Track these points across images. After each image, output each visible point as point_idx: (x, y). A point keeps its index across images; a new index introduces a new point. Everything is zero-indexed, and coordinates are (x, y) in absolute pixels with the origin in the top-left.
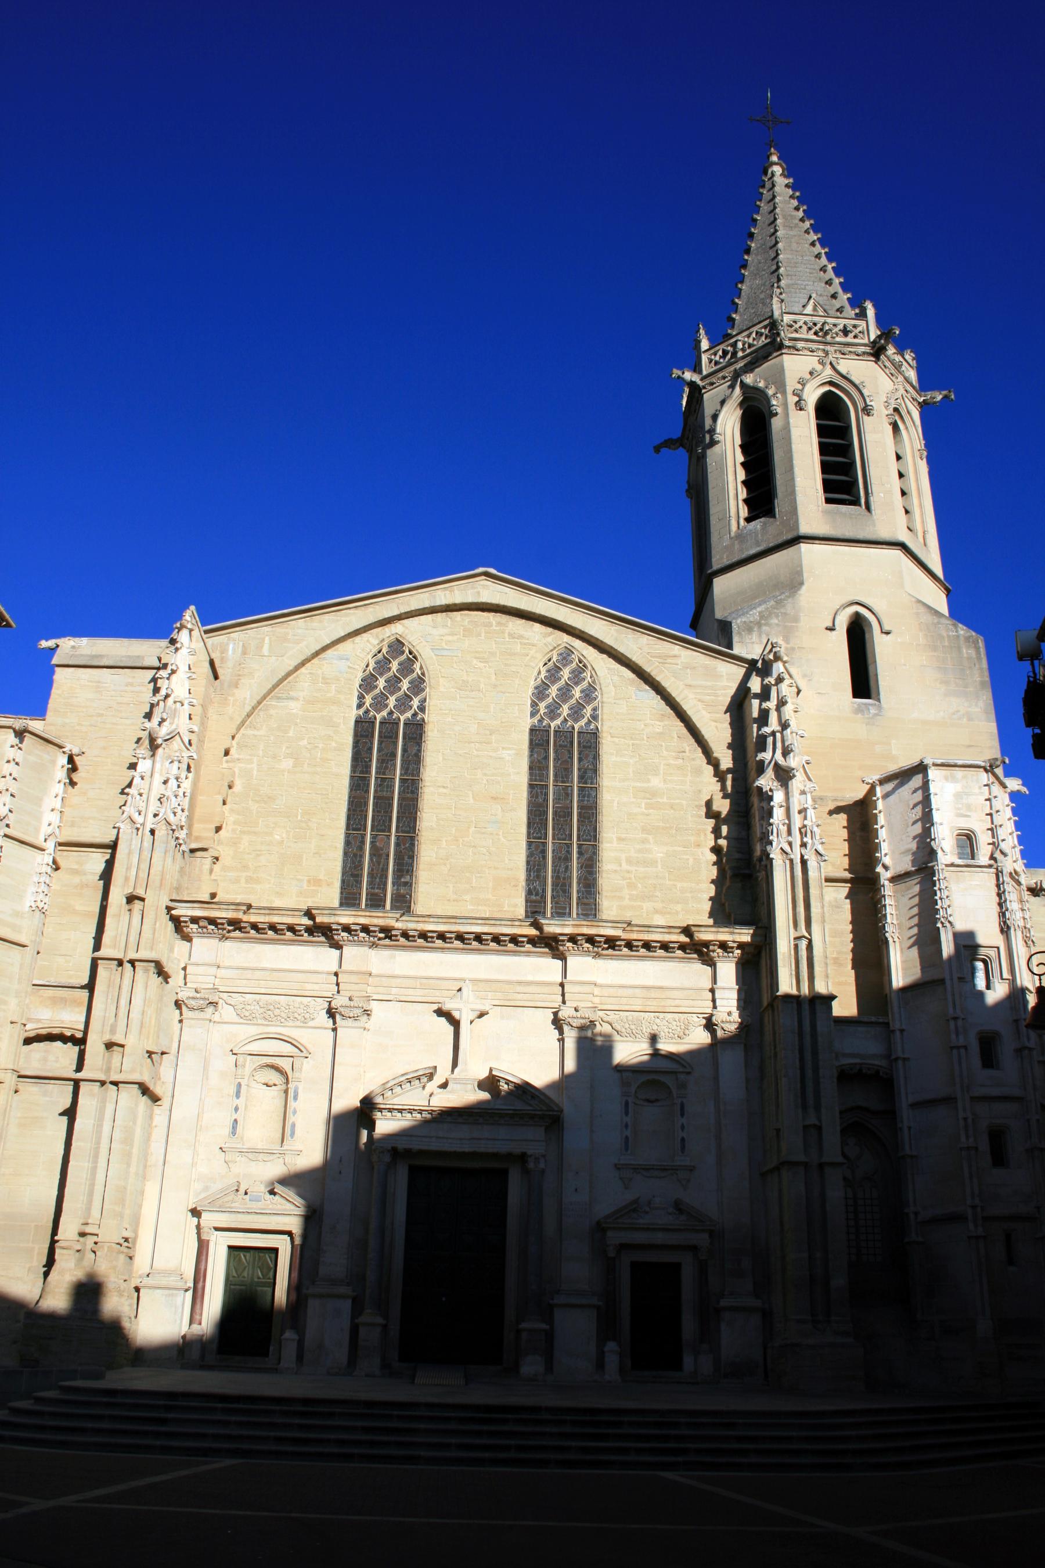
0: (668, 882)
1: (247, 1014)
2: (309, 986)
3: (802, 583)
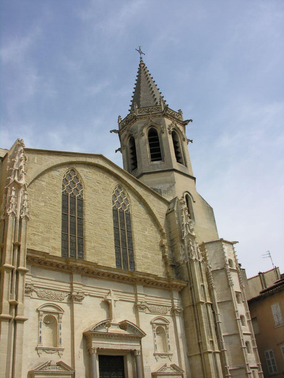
0: (153, 265)
1: (42, 295)
2: (62, 287)
3: (175, 183)
